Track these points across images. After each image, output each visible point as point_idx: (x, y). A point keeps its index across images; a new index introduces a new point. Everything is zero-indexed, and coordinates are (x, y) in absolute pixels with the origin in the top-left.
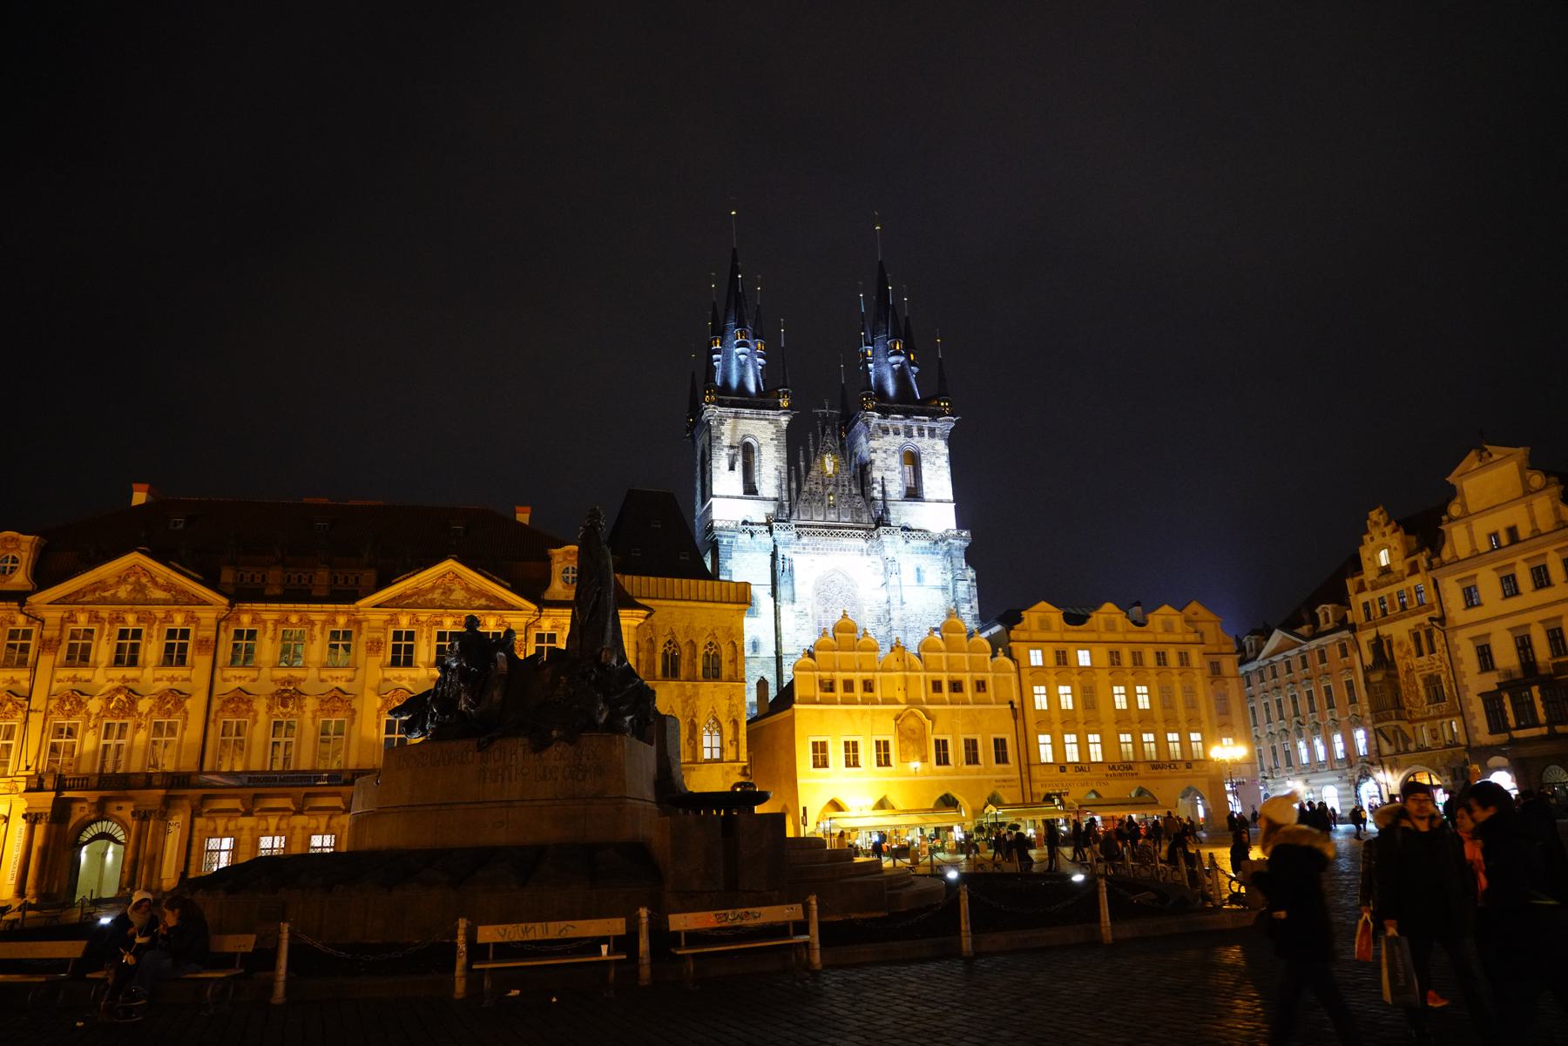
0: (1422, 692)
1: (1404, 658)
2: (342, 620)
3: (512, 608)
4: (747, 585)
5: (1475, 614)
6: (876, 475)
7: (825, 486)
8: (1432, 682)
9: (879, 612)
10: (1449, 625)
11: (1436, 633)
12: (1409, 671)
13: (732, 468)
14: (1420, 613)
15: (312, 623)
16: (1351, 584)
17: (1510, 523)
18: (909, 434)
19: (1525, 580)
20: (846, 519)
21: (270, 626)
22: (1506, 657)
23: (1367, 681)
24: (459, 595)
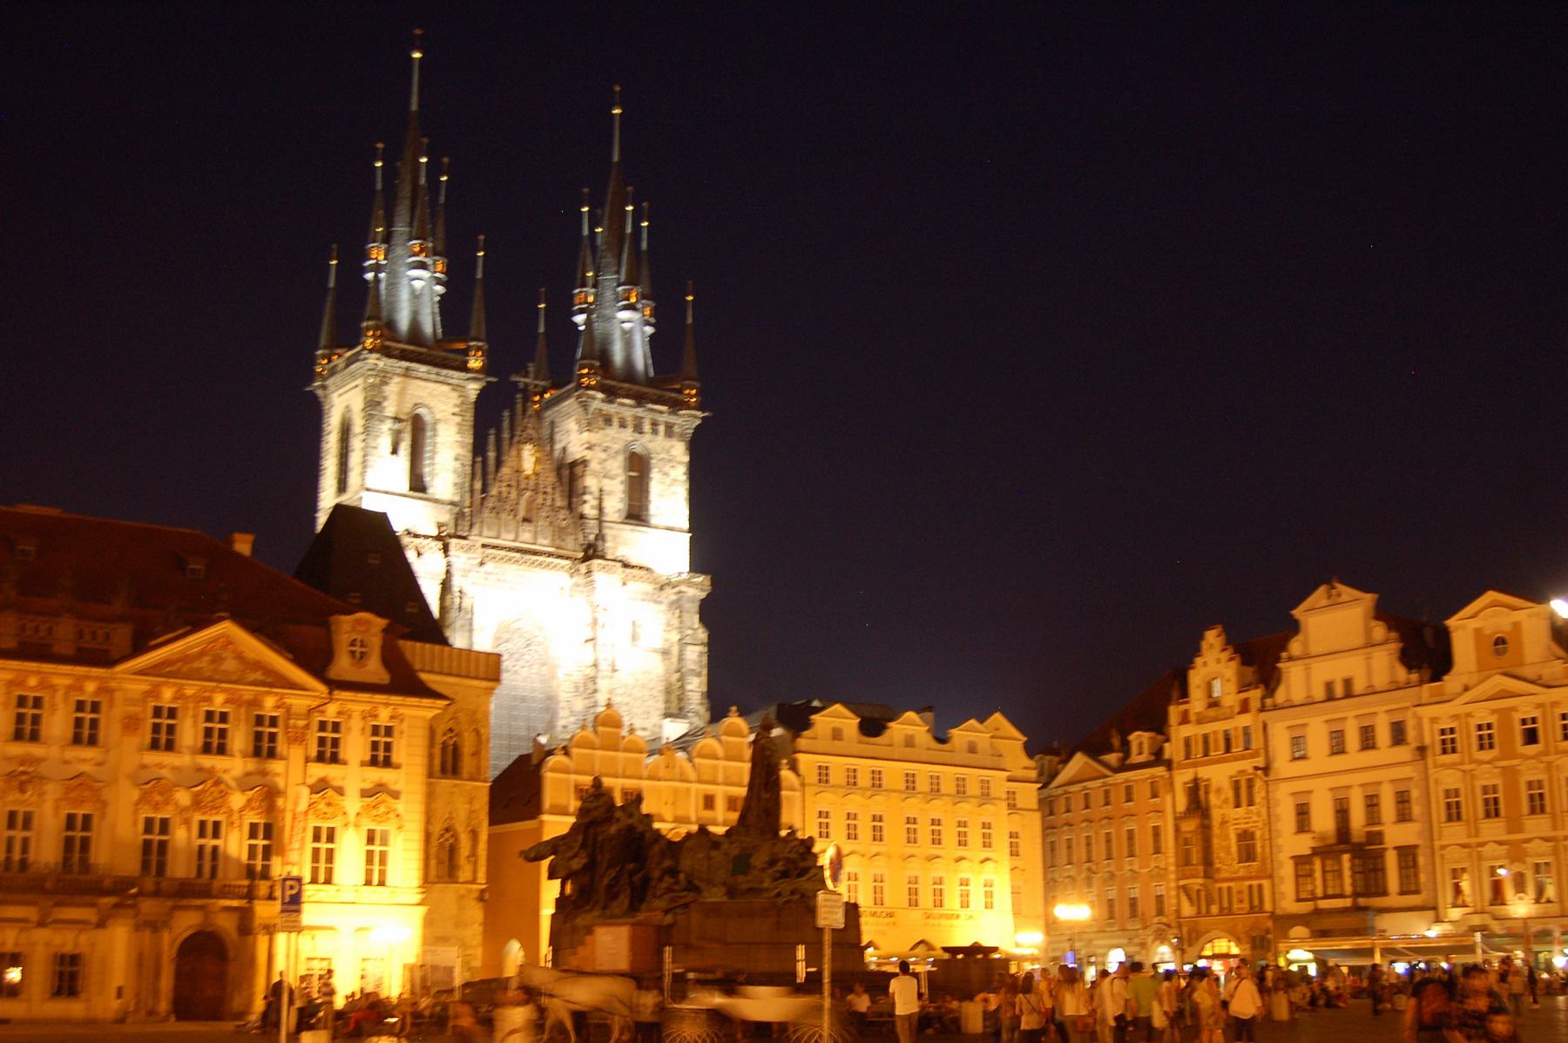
0: (1234, 849)
1: (1221, 807)
2: (91, 687)
3: (293, 685)
4: (499, 656)
5: (1300, 768)
6: (590, 482)
7: (520, 492)
8: (1246, 837)
9: (578, 677)
10: (1272, 777)
11: (1258, 784)
12: (1224, 823)
13: (395, 452)
14: (1243, 758)
15: (53, 688)
16: (1174, 712)
17: (1346, 674)
18: (638, 429)
19: (1352, 739)
20: (544, 543)
21: (60, 695)
22: (1323, 821)
23: (1177, 830)
24: (230, 665)
